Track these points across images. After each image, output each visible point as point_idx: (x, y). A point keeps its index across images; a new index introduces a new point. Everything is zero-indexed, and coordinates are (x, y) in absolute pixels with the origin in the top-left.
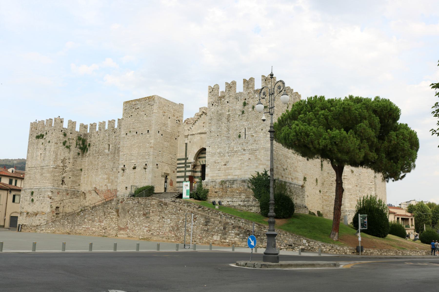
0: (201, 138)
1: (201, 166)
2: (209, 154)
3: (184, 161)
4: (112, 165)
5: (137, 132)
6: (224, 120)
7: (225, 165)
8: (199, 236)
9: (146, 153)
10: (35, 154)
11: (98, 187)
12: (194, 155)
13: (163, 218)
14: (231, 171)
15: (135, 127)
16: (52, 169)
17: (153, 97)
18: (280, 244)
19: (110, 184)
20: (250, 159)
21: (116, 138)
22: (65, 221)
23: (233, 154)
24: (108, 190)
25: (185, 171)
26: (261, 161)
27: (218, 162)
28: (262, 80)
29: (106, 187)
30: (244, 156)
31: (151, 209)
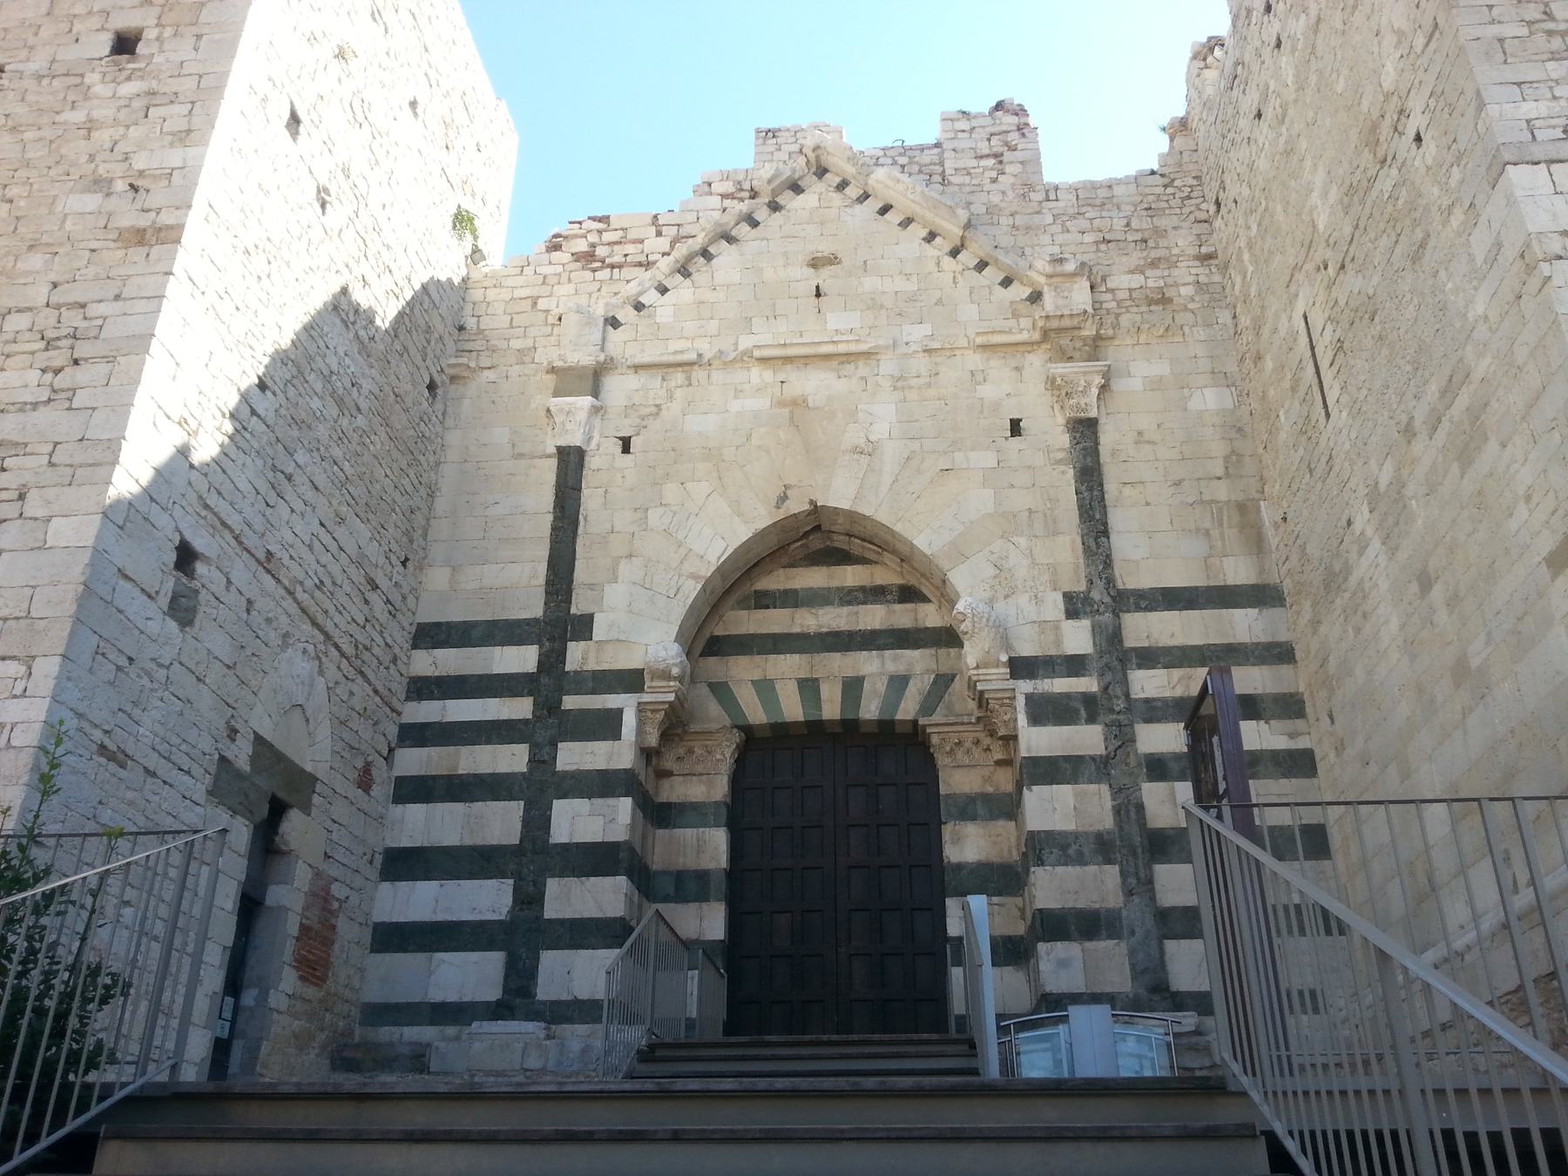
0: (797, 405)
1: (736, 737)
3: (522, 659)
12: (692, 590)
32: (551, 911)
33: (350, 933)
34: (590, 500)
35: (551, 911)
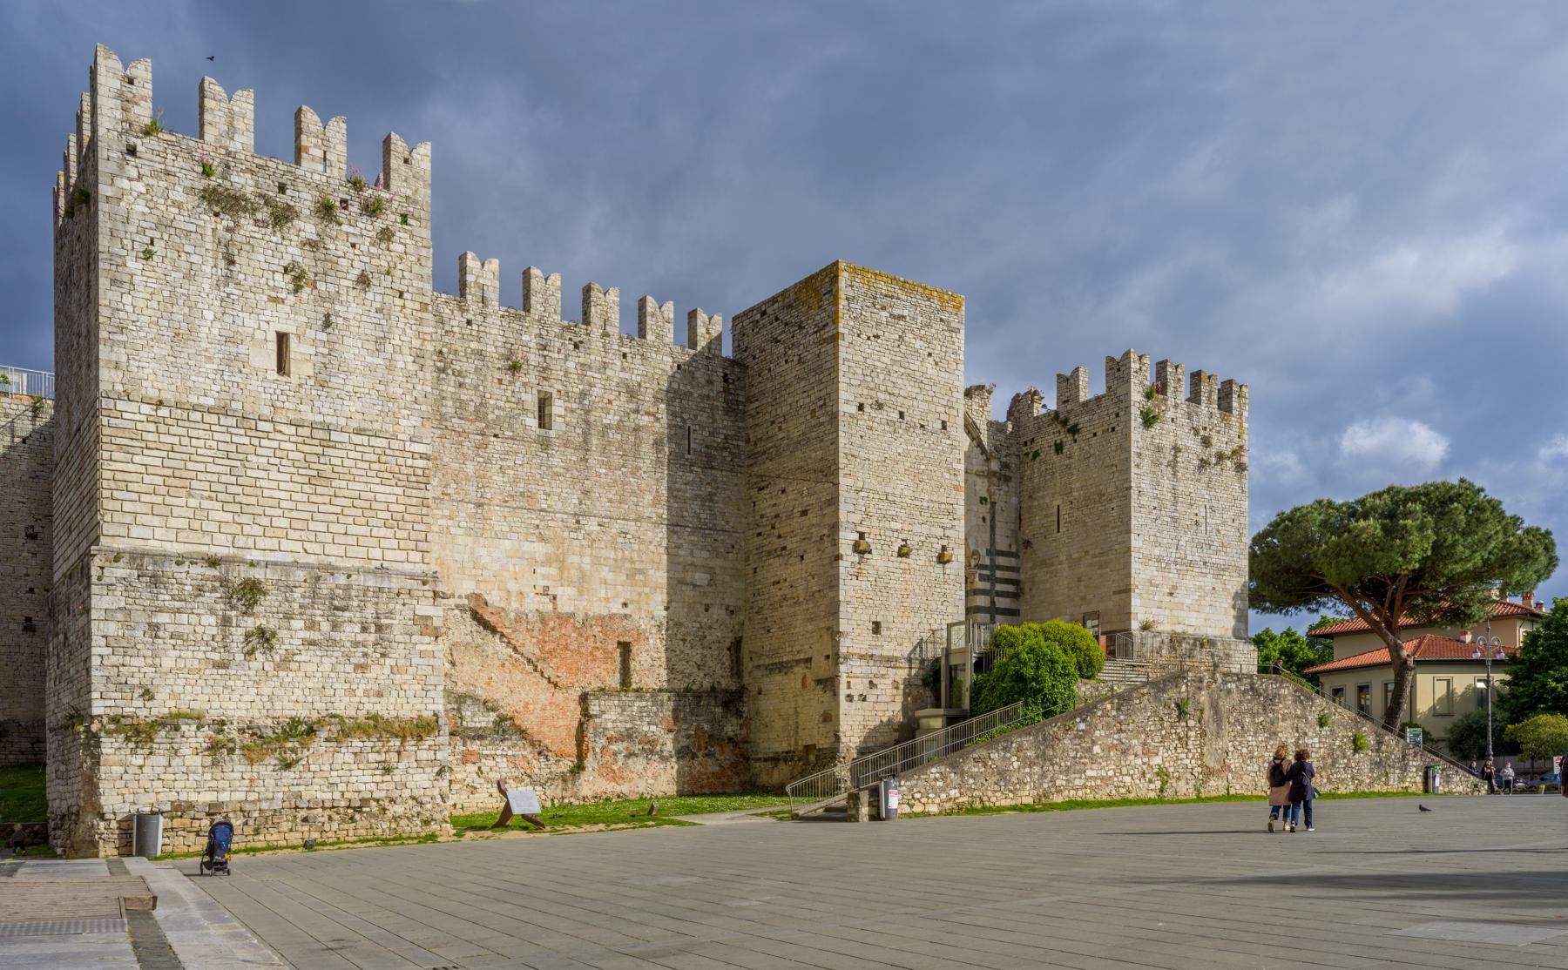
2: (1137, 555)
9: (943, 506)
10: (209, 315)
11: (494, 593)
19: (570, 591)
21: (589, 373)
22: (1009, 758)
24: (564, 619)
29: (546, 599)
30: (1205, 579)
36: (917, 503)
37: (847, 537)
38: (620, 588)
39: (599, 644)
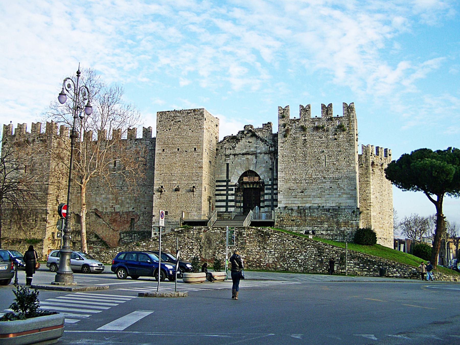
0: (248, 159)
2: (281, 179)
3: (225, 184)
4: (121, 183)
5: (178, 149)
6: (300, 144)
7: (302, 192)
8: (311, 266)
9: (194, 174)
13: (265, 248)
14: (310, 199)
15: (176, 143)
16: (47, 186)
17: (201, 110)
18: (404, 272)
19: (118, 206)
20: (331, 187)
23: (312, 181)
24: (117, 213)
25: (227, 195)
26: (345, 190)
27: (293, 188)
28: (344, 107)
29: (113, 208)
30: (324, 184)
31: (248, 239)
32: (229, 205)
33: (214, 206)
34: (230, 168)
35: (229, 205)
36: (183, 174)
37: (156, 187)
38: (132, 204)
39: (126, 219)
